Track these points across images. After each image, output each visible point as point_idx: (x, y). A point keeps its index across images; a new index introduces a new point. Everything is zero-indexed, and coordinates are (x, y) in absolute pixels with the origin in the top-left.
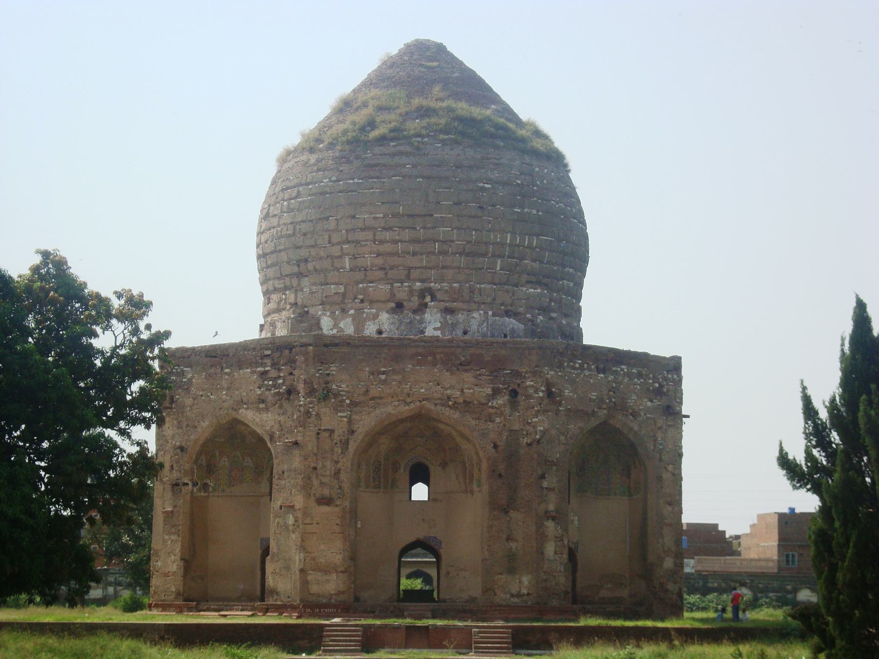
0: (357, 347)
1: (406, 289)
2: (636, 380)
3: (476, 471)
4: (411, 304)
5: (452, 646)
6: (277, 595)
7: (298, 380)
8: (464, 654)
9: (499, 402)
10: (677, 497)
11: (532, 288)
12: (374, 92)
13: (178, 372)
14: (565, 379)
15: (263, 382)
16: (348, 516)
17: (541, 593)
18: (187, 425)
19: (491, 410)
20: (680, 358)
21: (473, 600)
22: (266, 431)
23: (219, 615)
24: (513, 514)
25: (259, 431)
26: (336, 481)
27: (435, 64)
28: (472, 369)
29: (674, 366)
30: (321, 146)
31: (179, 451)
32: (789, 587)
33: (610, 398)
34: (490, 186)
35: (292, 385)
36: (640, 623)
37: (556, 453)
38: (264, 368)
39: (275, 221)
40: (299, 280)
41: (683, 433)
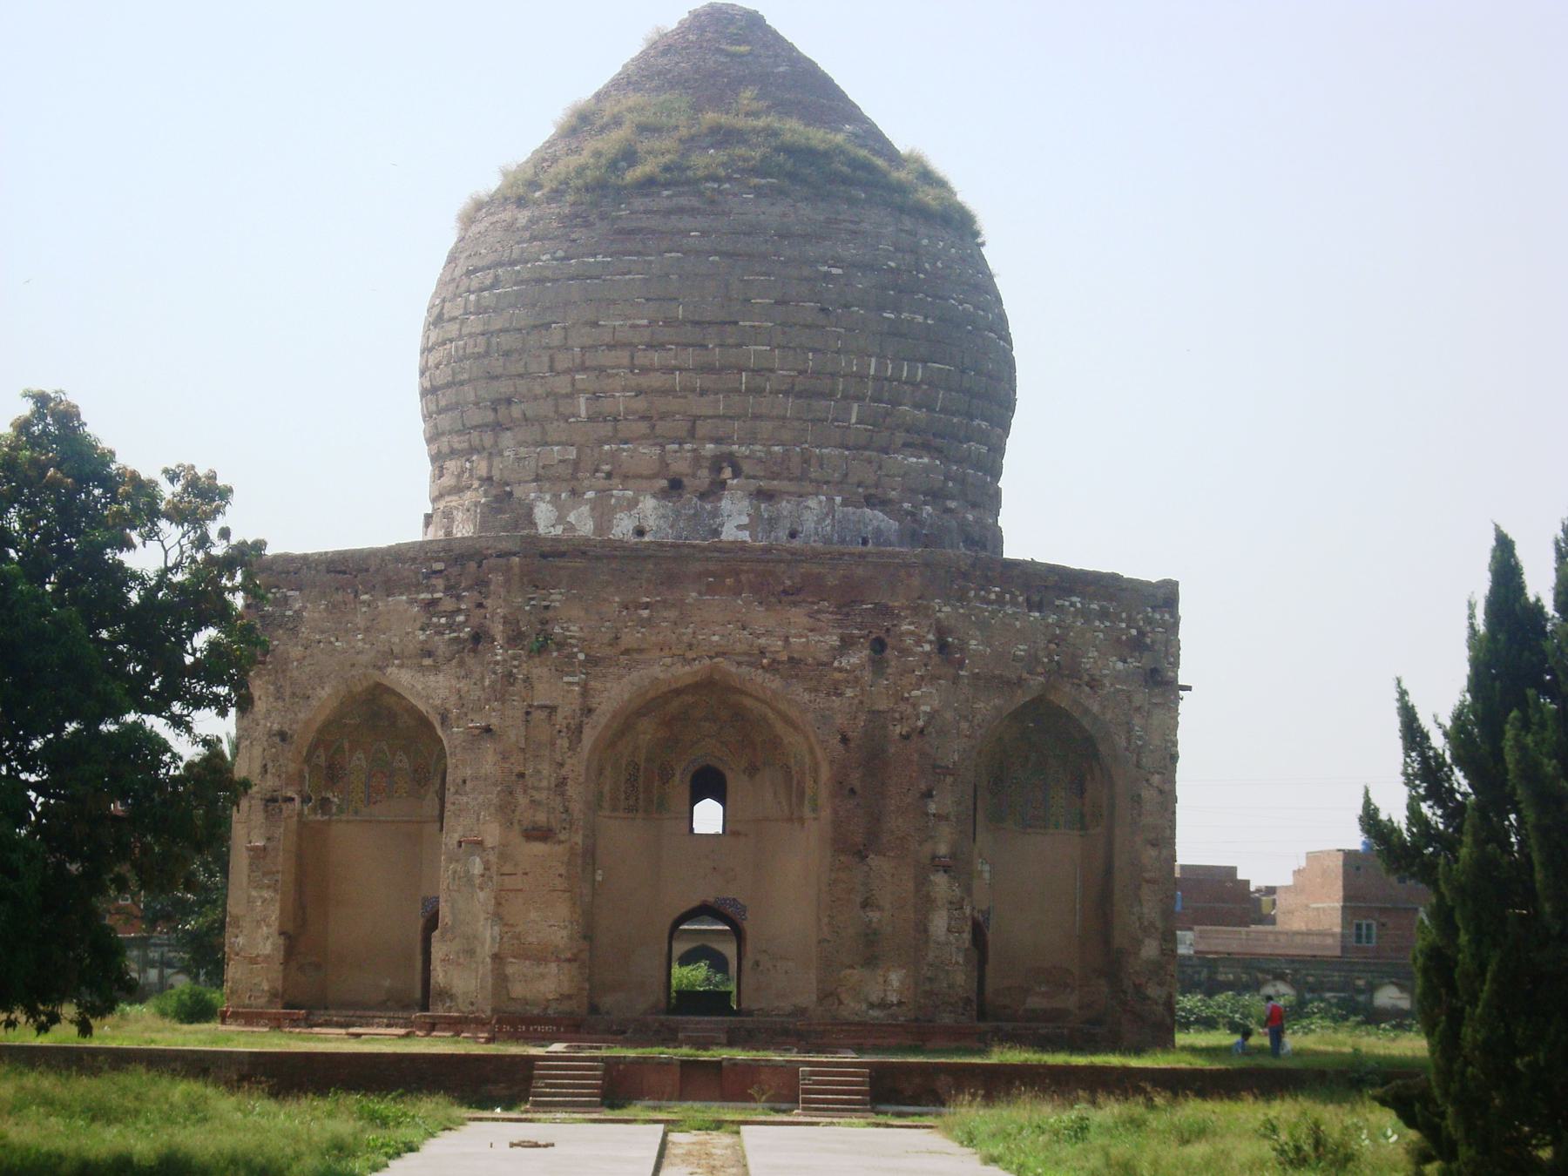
0: (598, 558)
1: (688, 454)
2: (1097, 623)
3: (809, 783)
4: (697, 482)
5: (764, 1098)
6: (452, 1000)
7: (492, 616)
8: (784, 1111)
10: (1168, 832)
11: (912, 456)
12: (633, 99)
13: (276, 598)
15: (431, 619)
16: (579, 861)
17: (922, 1001)
18: (294, 694)
19: (837, 675)
20: (1176, 584)
21: (800, 1012)
22: (435, 707)
23: (348, 1034)
24: (874, 861)
25: (422, 707)
26: (559, 799)
27: (743, 49)
28: (804, 601)
29: (1164, 597)
30: (538, 194)
31: (277, 739)
32: (1361, 983)
33: (1050, 656)
34: (840, 271)
35: (481, 625)
36: (1099, 1060)
37: (952, 753)
38: (432, 593)
39: (453, 329)
40: (496, 436)
41: (1180, 719)
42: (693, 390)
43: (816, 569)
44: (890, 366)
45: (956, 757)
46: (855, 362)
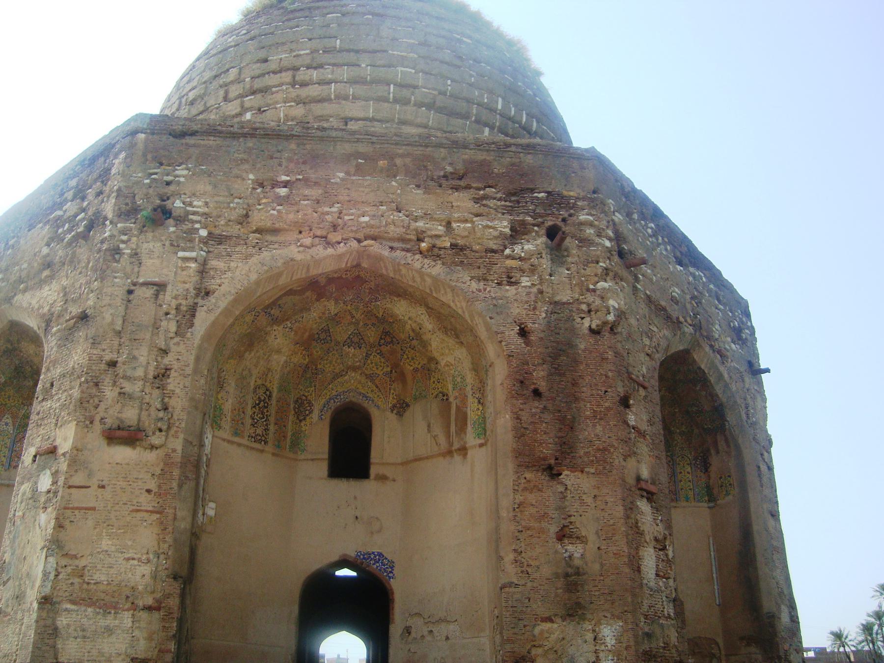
3: (472, 406)
9: (526, 247)
14: (638, 240)
16: (176, 473)
19: (510, 263)
24: (568, 477)
26: (156, 392)
28: (468, 187)
42: (346, 98)
43: (481, 156)
44: (513, 109)
45: (644, 370)
46: (486, 96)
